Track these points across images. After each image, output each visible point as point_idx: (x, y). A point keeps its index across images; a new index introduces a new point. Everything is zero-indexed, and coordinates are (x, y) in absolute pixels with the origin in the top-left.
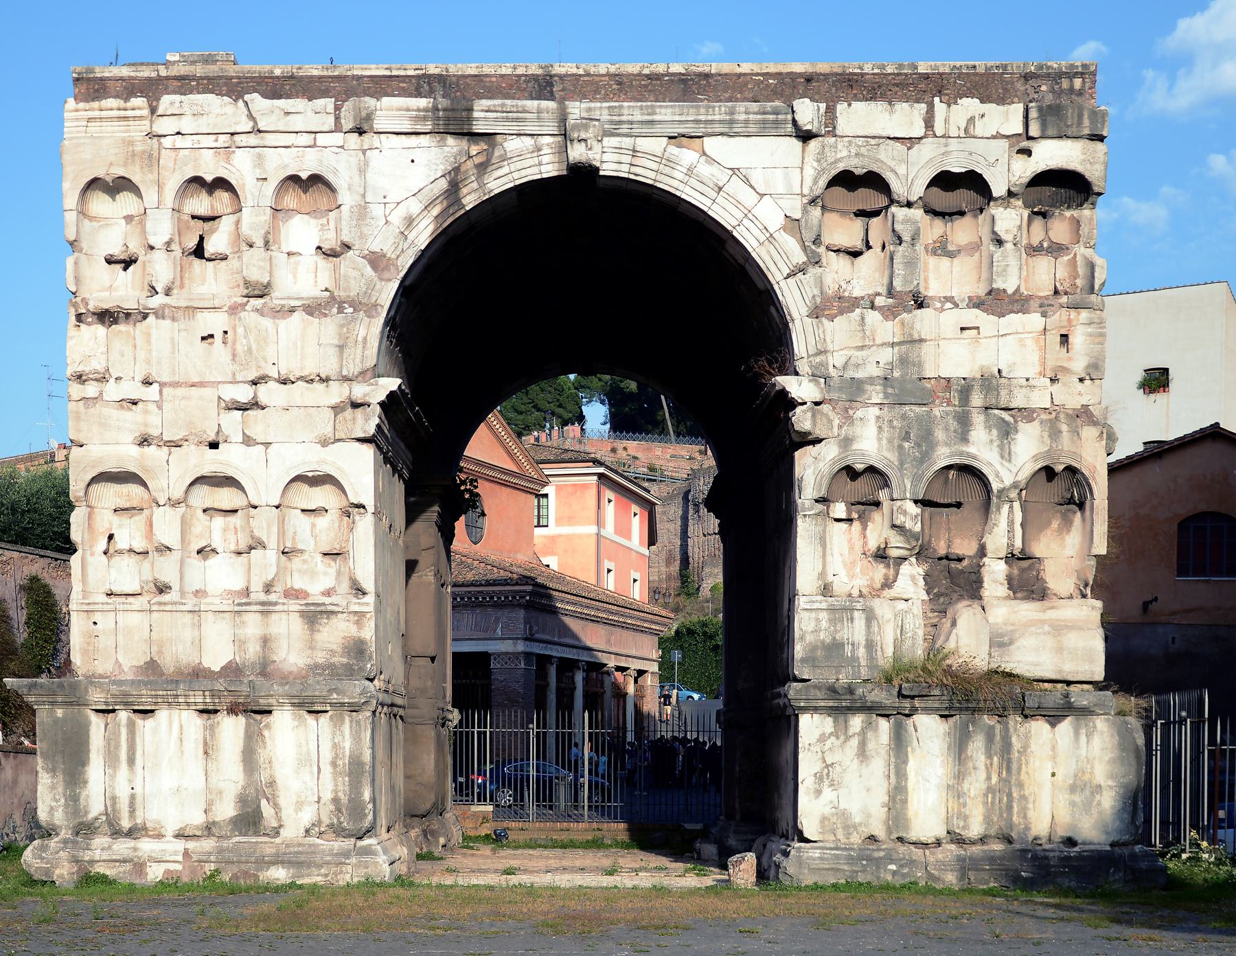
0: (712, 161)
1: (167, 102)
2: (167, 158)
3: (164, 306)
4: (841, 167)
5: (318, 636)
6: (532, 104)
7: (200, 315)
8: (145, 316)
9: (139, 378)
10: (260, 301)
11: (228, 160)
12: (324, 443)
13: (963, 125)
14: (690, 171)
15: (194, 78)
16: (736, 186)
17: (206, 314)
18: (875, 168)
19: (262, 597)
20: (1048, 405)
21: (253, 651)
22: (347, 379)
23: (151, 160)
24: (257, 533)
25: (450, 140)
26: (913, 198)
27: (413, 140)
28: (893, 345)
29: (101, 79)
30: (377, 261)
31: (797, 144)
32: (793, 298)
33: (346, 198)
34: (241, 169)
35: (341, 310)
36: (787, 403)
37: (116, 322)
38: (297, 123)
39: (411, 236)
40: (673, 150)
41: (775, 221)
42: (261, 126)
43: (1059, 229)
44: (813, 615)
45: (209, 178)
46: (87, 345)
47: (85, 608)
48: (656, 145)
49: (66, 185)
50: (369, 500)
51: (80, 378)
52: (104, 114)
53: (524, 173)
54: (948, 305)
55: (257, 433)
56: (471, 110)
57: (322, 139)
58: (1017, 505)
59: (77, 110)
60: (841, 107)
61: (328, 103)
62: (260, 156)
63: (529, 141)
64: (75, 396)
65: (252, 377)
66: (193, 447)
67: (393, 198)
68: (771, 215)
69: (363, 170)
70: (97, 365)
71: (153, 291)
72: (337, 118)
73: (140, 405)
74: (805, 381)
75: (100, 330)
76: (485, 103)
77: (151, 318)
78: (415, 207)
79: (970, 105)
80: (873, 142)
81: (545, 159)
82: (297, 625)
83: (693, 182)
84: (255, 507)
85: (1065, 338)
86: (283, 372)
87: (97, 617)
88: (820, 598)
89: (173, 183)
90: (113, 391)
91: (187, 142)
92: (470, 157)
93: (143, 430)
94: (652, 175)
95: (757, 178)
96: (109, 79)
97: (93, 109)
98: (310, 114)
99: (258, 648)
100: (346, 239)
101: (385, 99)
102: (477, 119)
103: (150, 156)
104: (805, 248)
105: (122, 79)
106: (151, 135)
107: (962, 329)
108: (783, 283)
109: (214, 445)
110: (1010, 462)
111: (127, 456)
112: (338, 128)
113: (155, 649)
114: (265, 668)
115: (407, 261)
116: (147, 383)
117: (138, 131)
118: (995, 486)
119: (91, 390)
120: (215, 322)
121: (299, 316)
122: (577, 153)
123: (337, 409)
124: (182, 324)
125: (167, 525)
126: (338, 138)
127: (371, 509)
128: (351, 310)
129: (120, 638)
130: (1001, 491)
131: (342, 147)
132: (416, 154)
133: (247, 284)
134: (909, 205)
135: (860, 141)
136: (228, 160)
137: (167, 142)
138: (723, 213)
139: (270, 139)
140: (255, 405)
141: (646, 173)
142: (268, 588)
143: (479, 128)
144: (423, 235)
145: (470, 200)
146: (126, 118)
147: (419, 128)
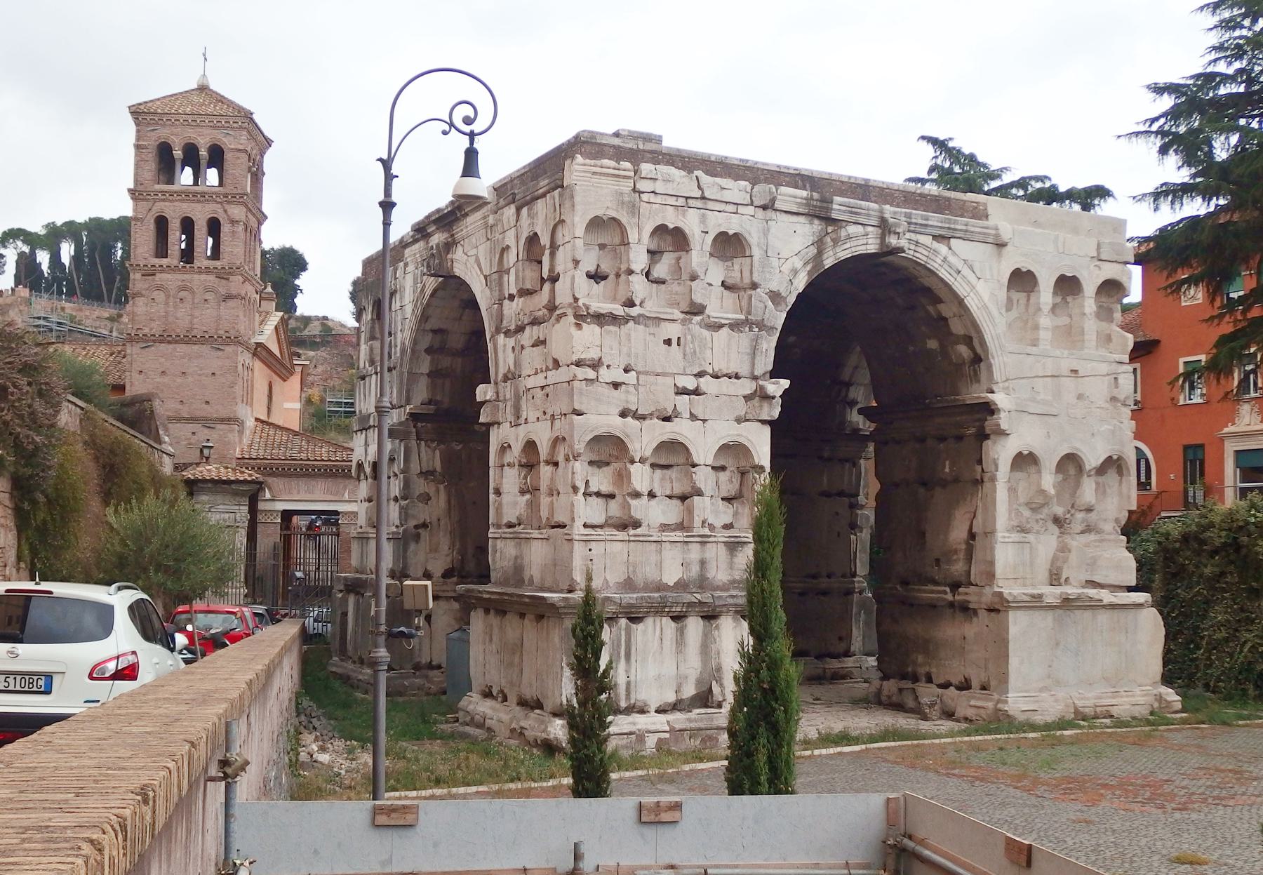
0: (954, 254)
1: (646, 168)
2: (644, 208)
3: (640, 315)
5: (736, 560)
7: (663, 324)
10: (698, 318)
11: (684, 215)
12: (739, 420)
15: (660, 153)
16: (966, 271)
17: (667, 324)
21: (695, 570)
22: (755, 378)
23: (634, 209)
24: (698, 484)
25: (816, 222)
29: (600, 144)
30: (775, 297)
33: (757, 253)
34: (691, 223)
35: (750, 330)
36: (989, 409)
38: (727, 196)
39: (795, 282)
40: (936, 245)
42: (707, 195)
45: (671, 226)
46: (588, 340)
48: (927, 240)
49: (577, 219)
50: (766, 462)
51: (578, 364)
61: (744, 184)
62: (703, 215)
64: (580, 377)
67: (784, 255)
69: (766, 232)
70: (593, 354)
71: (630, 303)
75: (597, 329)
77: (631, 324)
78: (799, 264)
81: (870, 241)
82: (722, 550)
83: (946, 266)
84: (694, 466)
87: (592, 545)
89: (648, 228)
90: (606, 375)
91: (659, 199)
95: (977, 267)
96: (605, 145)
98: (736, 191)
99: (698, 568)
100: (756, 279)
101: (783, 189)
103: (634, 206)
105: (614, 146)
109: (667, 419)
111: (612, 423)
113: (631, 569)
114: (703, 583)
115: (792, 300)
116: (626, 371)
118: (1088, 467)
119: (591, 374)
120: (673, 331)
121: (725, 330)
122: (893, 241)
123: (747, 398)
124: (652, 330)
125: (641, 477)
126: (751, 210)
127: (768, 470)
129: (608, 561)
132: (798, 228)
133: (692, 303)
136: (684, 215)
137: (645, 197)
138: (960, 288)
139: (711, 205)
140: (697, 392)
141: (921, 256)
143: (834, 216)
144: (801, 283)
145: (829, 262)
146: (618, 176)
147: (801, 210)
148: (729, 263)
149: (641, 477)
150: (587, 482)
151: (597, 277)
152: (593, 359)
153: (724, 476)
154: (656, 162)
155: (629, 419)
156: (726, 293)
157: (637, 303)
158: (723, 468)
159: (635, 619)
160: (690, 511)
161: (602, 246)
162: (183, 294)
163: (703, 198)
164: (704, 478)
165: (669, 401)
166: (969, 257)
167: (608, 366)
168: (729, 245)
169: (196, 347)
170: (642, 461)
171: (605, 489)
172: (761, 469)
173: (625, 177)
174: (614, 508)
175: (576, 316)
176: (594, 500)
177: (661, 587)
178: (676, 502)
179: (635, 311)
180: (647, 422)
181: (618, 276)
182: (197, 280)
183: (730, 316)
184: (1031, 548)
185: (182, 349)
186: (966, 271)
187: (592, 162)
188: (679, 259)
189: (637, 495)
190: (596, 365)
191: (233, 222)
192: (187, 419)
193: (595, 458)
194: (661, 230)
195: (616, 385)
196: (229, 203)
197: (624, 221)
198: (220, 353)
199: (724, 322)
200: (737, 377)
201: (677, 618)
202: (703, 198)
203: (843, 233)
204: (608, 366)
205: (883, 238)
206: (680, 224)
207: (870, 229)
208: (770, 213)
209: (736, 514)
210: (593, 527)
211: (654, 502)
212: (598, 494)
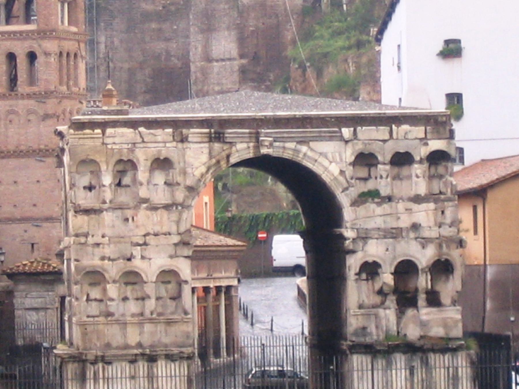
0: (312, 150)
1: (109, 131)
4: (360, 151)
6: (247, 131)
8: (102, 212)
9: (100, 235)
12: (171, 257)
13: (403, 135)
14: (305, 155)
16: (321, 160)
18: (372, 152)
19: (150, 316)
20: (438, 236)
22: (179, 234)
26: (386, 162)
27: (202, 145)
28: (381, 216)
31: (342, 144)
32: (344, 200)
35: (177, 208)
36: (343, 238)
37: (91, 214)
38: (159, 139)
40: (299, 147)
41: (336, 172)
42: (145, 140)
43: (441, 170)
44: (356, 317)
47: (82, 323)
48: (291, 145)
52: (85, 136)
53: (244, 156)
54: (400, 201)
55: (146, 254)
56: (223, 134)
57: (168, 145)
58: (429, 274)
59: (74, 135)
60: (359, 128)
61: (170, 130)
63: (245, 145)
65: (143, 233)
66: (122, 261)
68: (334, 169)
69: (184, 156)
70: (85, 230)
71: (104, 202)
72: (173, 136)
73: (101, 246)
74: (349, 230)
76: (230, 131)
77: (105, 212)
78: (203, 169)
79: (405, 127)
80: (370, 142)
84: (146, 283)
85: (443, 212)
86: (156, 232)
87: (87, 327)
88: (358, 310)
92: (224, 150)
93: (102, 255)
94: (291, 156)
95: (330, 156)
97: (80, 134)
101: (192, 130)
102: (226, 137)
104: (348, 182)
106: (103, 143)
107: (406, 210)
108: (340, 195)
109: (129, 260)
110: (424, 257)
112: (174, 140)
116: (103, 237)
117: (98, 142)
118: (420, 267)
119: (83, 240)
121: (159, 211)
123: (176, 245)
126: (174, 144)
128: (180, 208)
130: (422, 269)
131: (176, 147)
134: (384, 164)
135: (367, 142)
137: (109, 147)
139: (149, 145)
140: (145, 244)
141: (288, 155)
142: (152, 313)
143: (228, 140)
148: (167, 172)
149: (112, 290)
150: (88, 295)
151: (90, 188)
152: (84, 233)
153: (170, 286)
154: (114, 127)
155: (106, 261)
156: (166, 188)
157: (108, 201)
158: (169, 282)
159: (109, 363)
160: (144, 306)
161: (92, 172)
162: (11, 117)
163: (143, 142)
164: (150, 289)
165: (128, 250)
166: (325, 151)
167: (93, 236)
168: (162, 163)
169: (23, 160)
170: (114, 282)
171: (98, 297)
172: (186, 282)
173: (97, 138)
174: (103, 307)
175: (76, 212)
176: (94, 304)
177: (127, 347)
178: (140, 302)
179: (106, 206)
180: (115, 262)
181: (100, 187)
182: (22, 105)
183: (163, 202)
184: (376, 318)
185: (12, 162)
186: (321, 160)
187: (80, 132)
188: (135, 175)
189: (112, 300)
190: (86, 235)
191: (47, 54)
192: (19, 220)
193: (91, 281)
194: (120, 161)
195: (98, 245)
196: (42, 38)
197: (98, 160)
198: (42, 164)
199: (159, 206)
200: (170, 234)
201: (133, 362)
202: (143, 142)
203: (234, 149)
204: (93, 236)
205: (257, 147)
206: (131, 157)
207: (251, 144)
208: (185, 145)
209: (176, 307)
210: (93, 317)
211: (128, 302)
212: (96, 300)
